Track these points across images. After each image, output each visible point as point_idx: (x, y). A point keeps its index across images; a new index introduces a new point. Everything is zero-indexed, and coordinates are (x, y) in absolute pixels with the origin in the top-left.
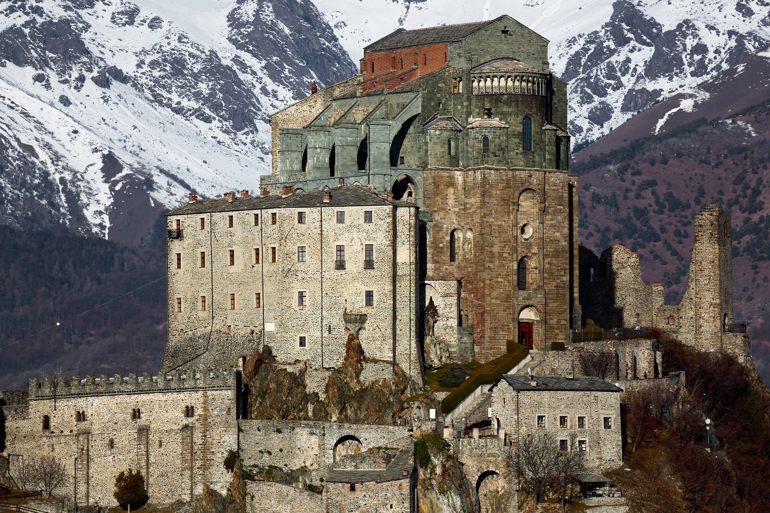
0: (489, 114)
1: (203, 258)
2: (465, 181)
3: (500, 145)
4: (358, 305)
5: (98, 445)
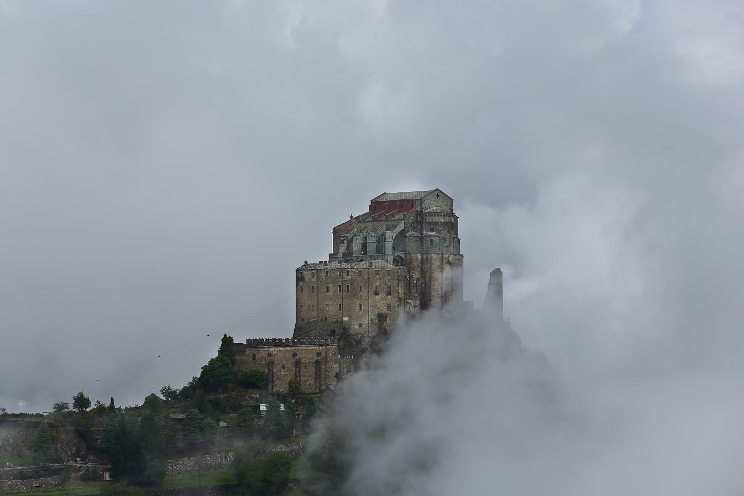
0: (432, 230)
1: (313, 288)
2: (422, 258)
3: (437, 243)
4: (384, 310)
5: (277, 368)
